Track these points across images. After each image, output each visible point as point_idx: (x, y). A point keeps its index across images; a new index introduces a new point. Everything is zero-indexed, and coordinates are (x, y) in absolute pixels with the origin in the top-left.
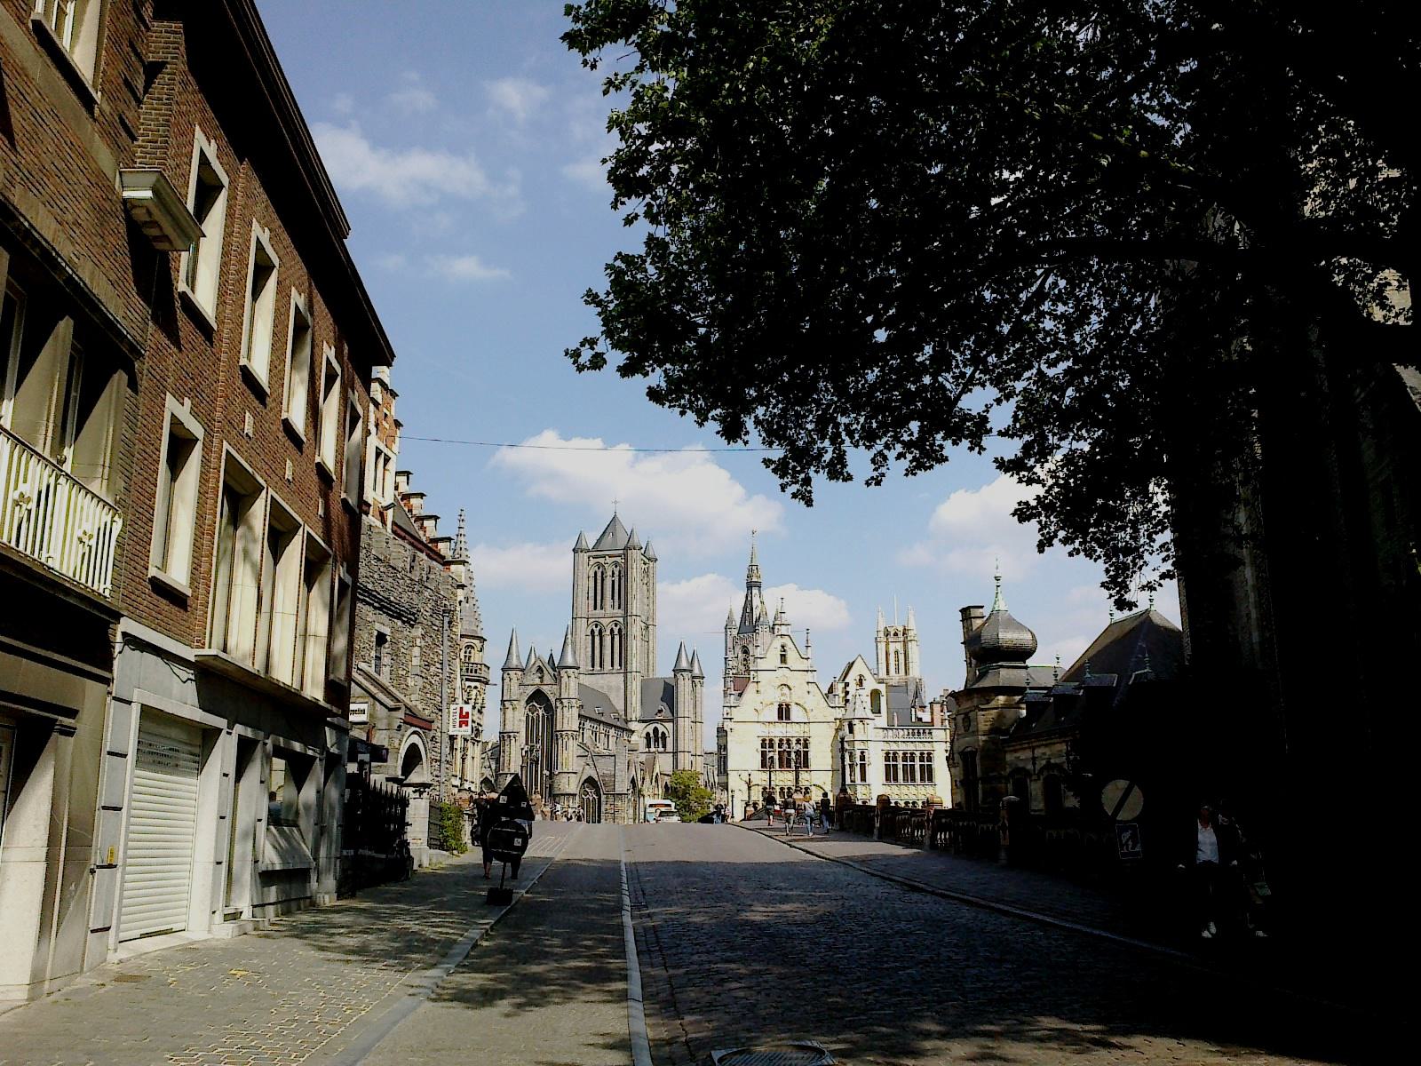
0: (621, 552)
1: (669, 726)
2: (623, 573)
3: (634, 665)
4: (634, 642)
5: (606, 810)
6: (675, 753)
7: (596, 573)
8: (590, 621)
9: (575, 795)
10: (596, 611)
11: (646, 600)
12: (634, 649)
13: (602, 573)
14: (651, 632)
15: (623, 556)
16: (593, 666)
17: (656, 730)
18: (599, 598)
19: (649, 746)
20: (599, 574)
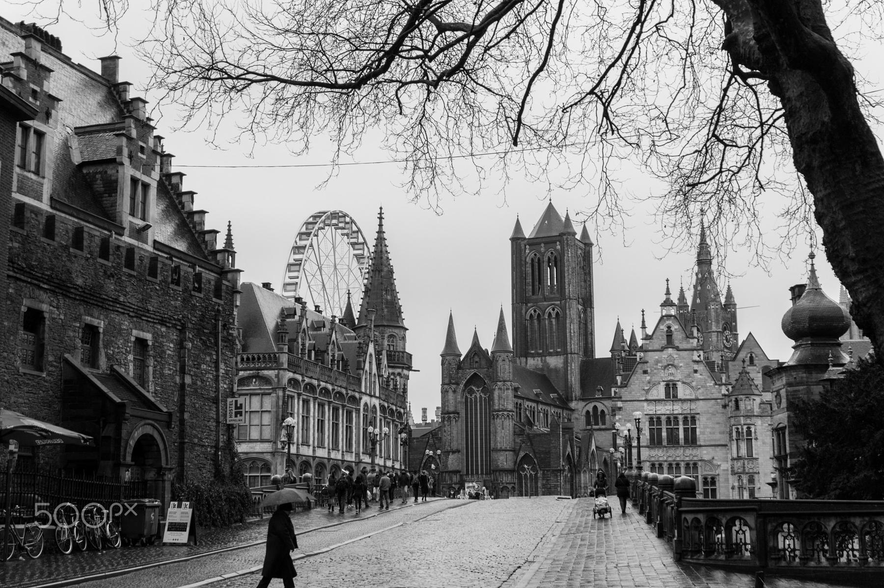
0: (554, 239)
2: (558, 258)
11: (583, 283)
13: (539, 259)
15: (558, 243)
17: (595, 408)
19: (588, 423)
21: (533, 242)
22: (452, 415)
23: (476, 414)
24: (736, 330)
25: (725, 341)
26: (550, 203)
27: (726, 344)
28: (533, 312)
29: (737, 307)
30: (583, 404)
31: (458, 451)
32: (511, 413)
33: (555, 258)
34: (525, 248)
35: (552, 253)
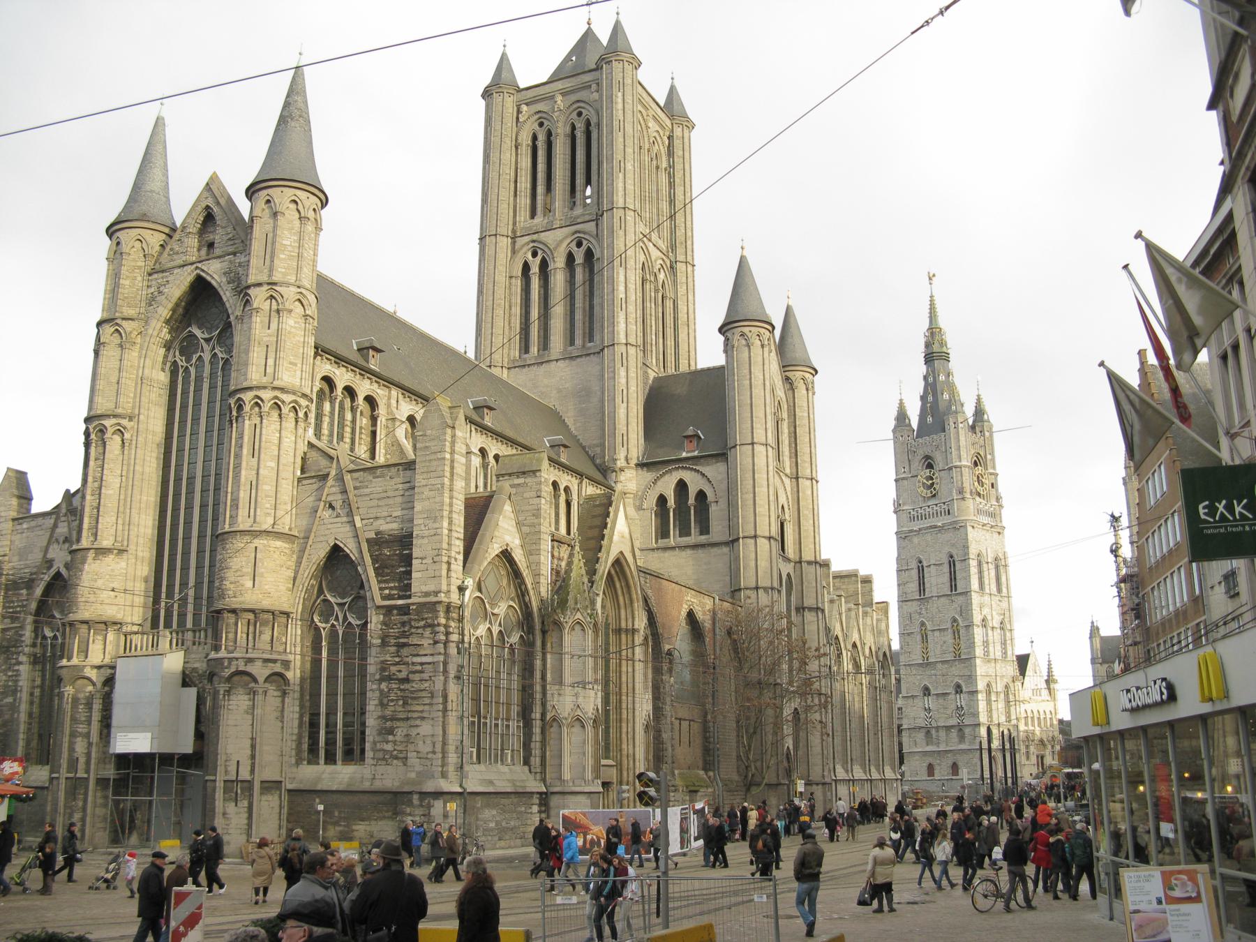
1: (714, 470)
2: (593, 121)
3: (621, 327)
4: (622, 271)
5: (384, 667)
6: (733, 542)
7: (535, 138)
8: (520, 241)
9: (287, 614)
10: (539, 219)
12: (622, 288)
14: (681, 278)
15: (594, 87)
16: (525, 348)
18: (541, 189)
20: (541, 138)
21: (535, 95)
22: (107, 423)
23: (196, 420)
24: (994, 468)
25: (976, 484)
26: (589, 29)
27: (979, 489)
28: (529, 256)
29: (994, 430)
30: (648, 476)
31: (121, 551)
32: (288, 398)
33: (588, 124)
34: (519, 112)
35: (580, 114)
